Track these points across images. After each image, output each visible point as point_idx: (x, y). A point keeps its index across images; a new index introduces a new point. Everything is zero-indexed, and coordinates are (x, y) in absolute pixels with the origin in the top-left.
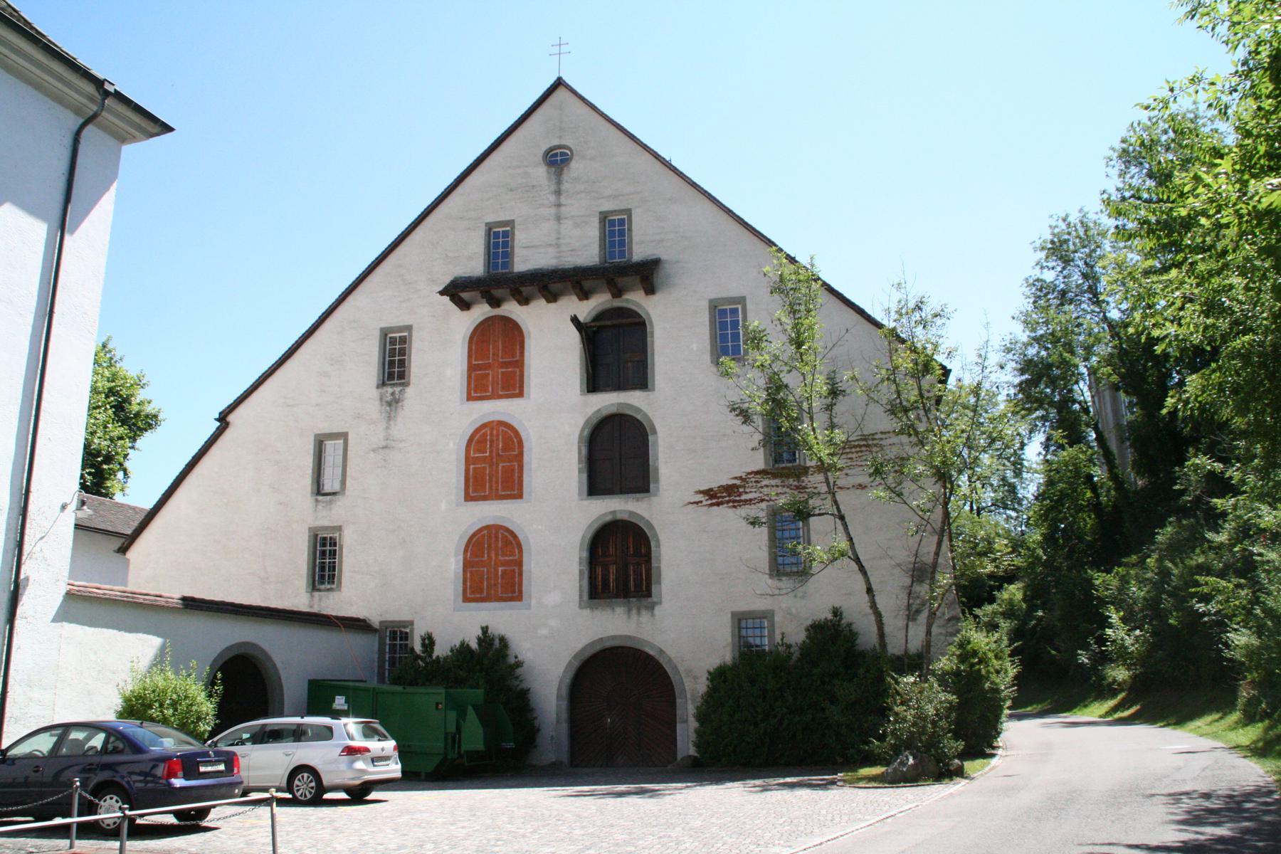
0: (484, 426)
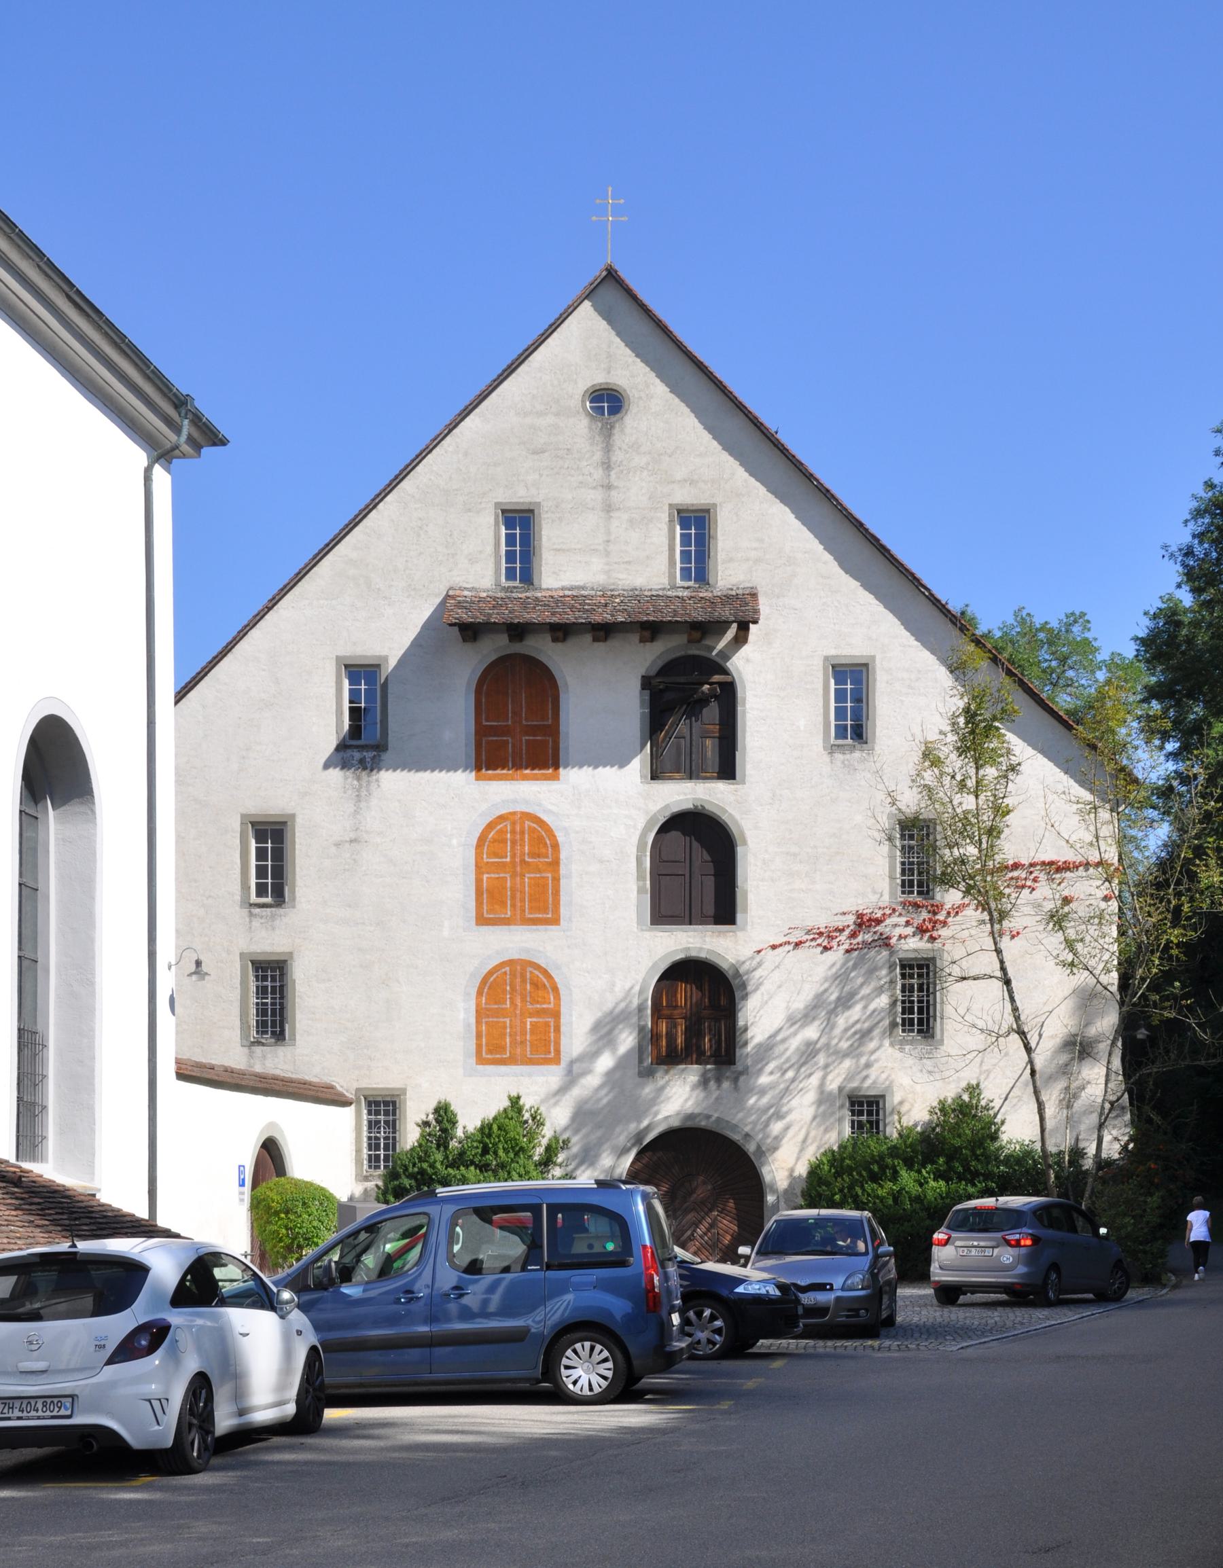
0: (501, 818)
